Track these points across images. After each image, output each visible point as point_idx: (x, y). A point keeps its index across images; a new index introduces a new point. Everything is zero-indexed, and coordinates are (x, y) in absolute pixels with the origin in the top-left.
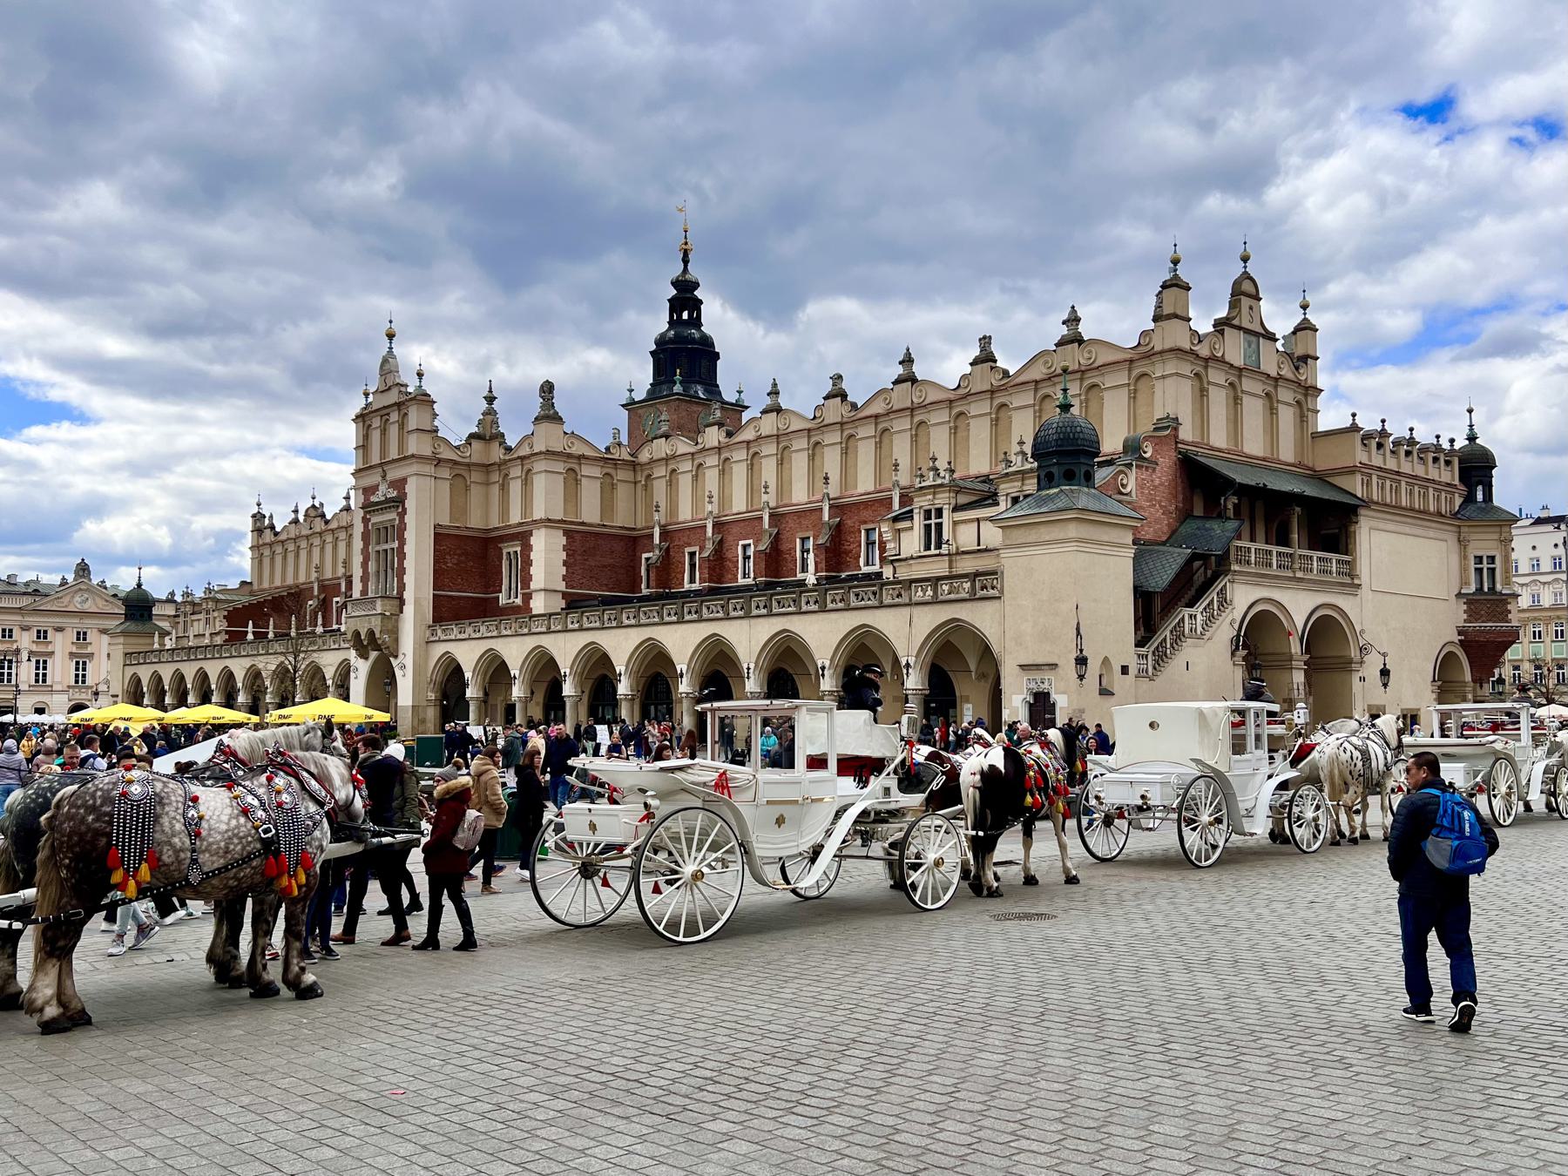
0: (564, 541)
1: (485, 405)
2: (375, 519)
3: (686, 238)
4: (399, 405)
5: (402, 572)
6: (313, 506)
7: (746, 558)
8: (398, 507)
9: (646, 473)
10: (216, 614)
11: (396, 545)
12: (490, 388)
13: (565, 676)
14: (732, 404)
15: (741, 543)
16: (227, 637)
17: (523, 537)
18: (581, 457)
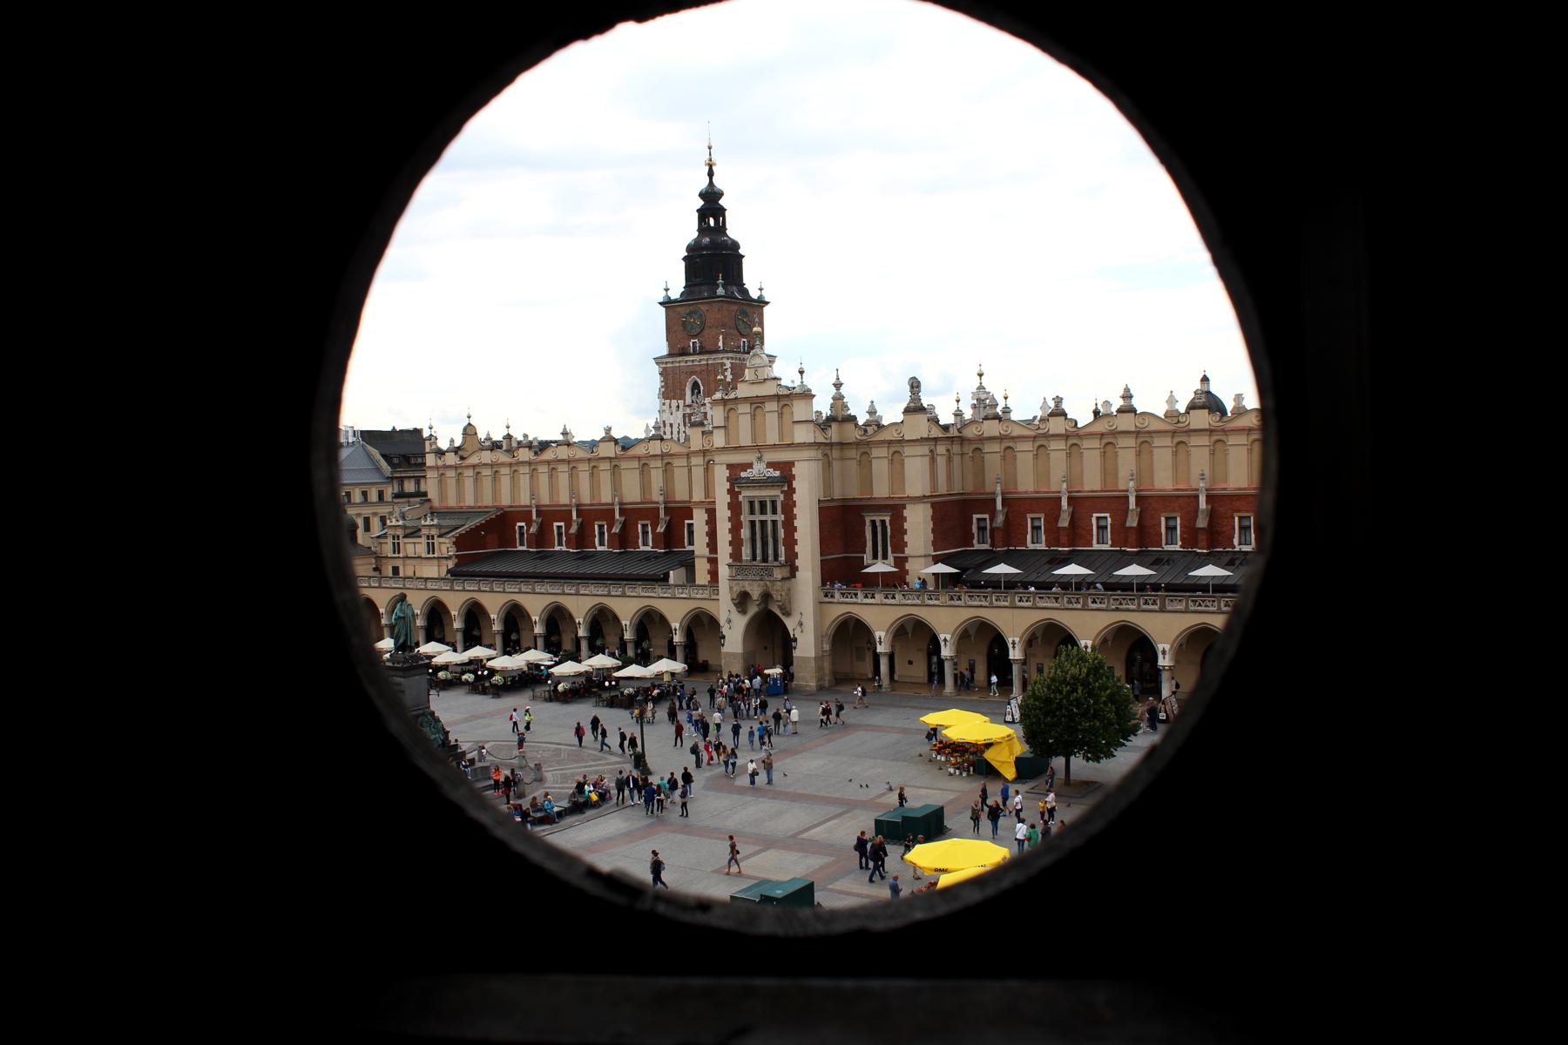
0: (930, 512)
1: (833, 391)
2: (745, 494)
3: (710, 154)
4: (778, 397)
5: (791, 542)
6: (469, 424)
7: (1102, 528)
8: (782, 486)
9: (975, 446)
10: (442, 540)
11: (780, 517)
12: (838, 376)
13: (1014, 643)
14: (753, 300)
15: (1095, 515)
16: (456, 560)
17: (896, 510)
18: (936, 440)
